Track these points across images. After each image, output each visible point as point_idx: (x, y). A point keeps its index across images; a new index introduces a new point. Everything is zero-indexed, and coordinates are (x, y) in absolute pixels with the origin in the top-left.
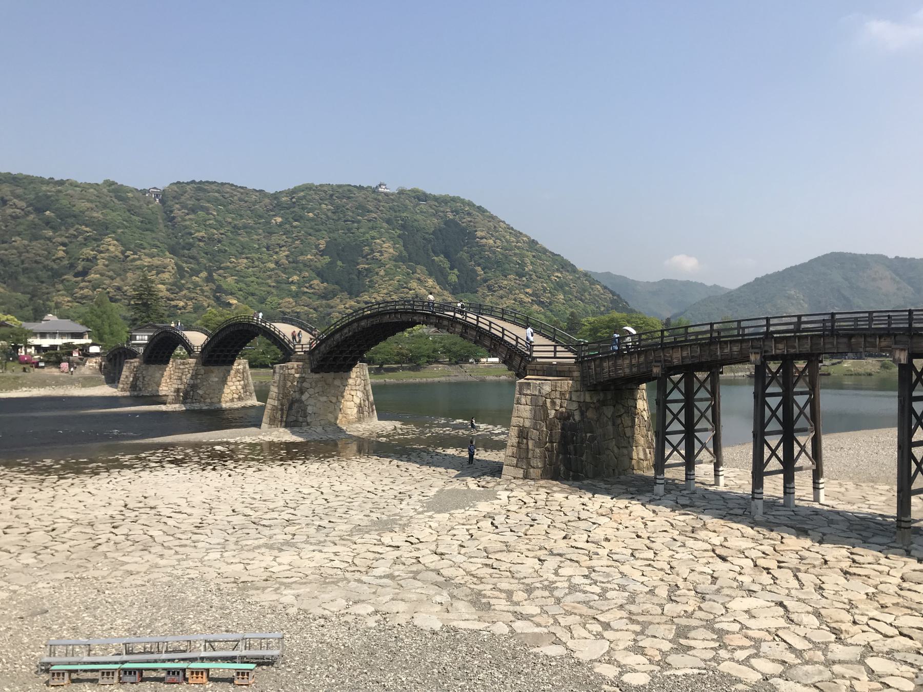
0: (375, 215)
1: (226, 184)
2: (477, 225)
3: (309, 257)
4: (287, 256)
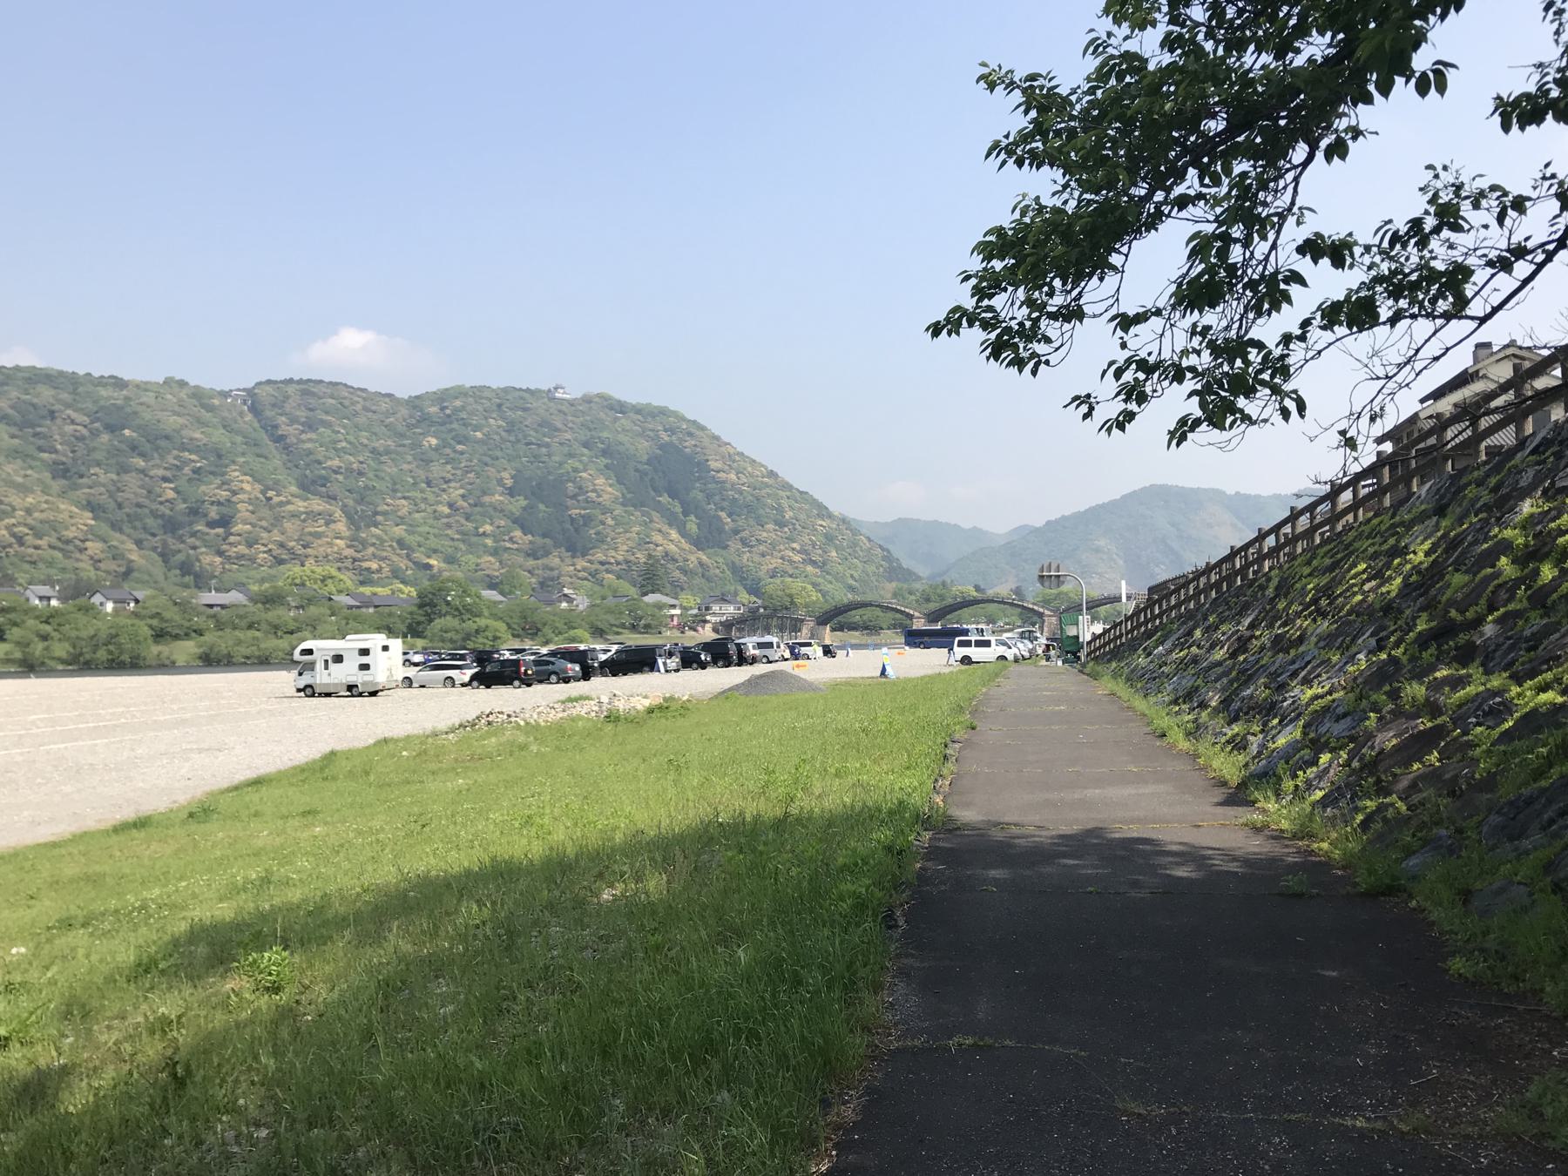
0: (568, 436)
1: (337, 384)
4: (463, 496)
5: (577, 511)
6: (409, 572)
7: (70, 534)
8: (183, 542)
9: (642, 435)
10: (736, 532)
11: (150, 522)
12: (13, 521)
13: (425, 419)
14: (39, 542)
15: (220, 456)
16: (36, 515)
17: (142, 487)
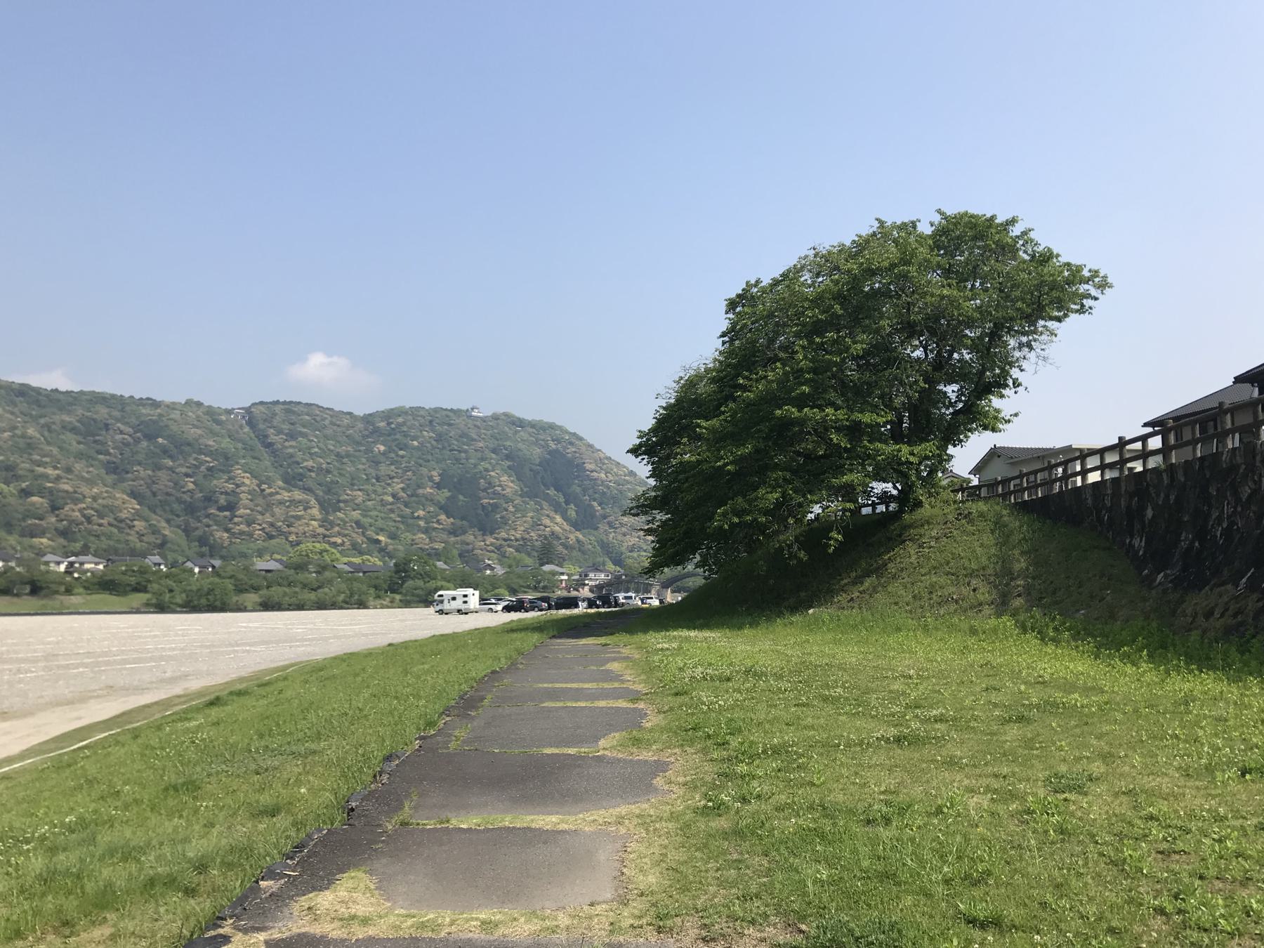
1: (311, 405)
2: (584, 457)
3: (429, 490)
4: (403, 489)
5: (487, 501)
6: (364, 546)
7: (123, 515)
8: (200, 521)
9: (536, 443)
10: (605, 517)
11: (176, 506)
12: (84, 505)
13: (376, 431)
14: (102, 521)
15: (227, 459)
16: (100, 501)
17: (170, 481)
